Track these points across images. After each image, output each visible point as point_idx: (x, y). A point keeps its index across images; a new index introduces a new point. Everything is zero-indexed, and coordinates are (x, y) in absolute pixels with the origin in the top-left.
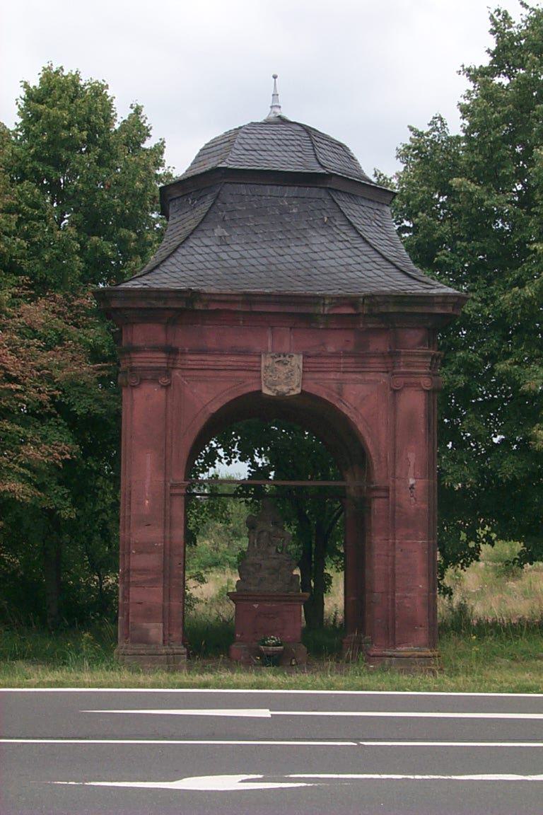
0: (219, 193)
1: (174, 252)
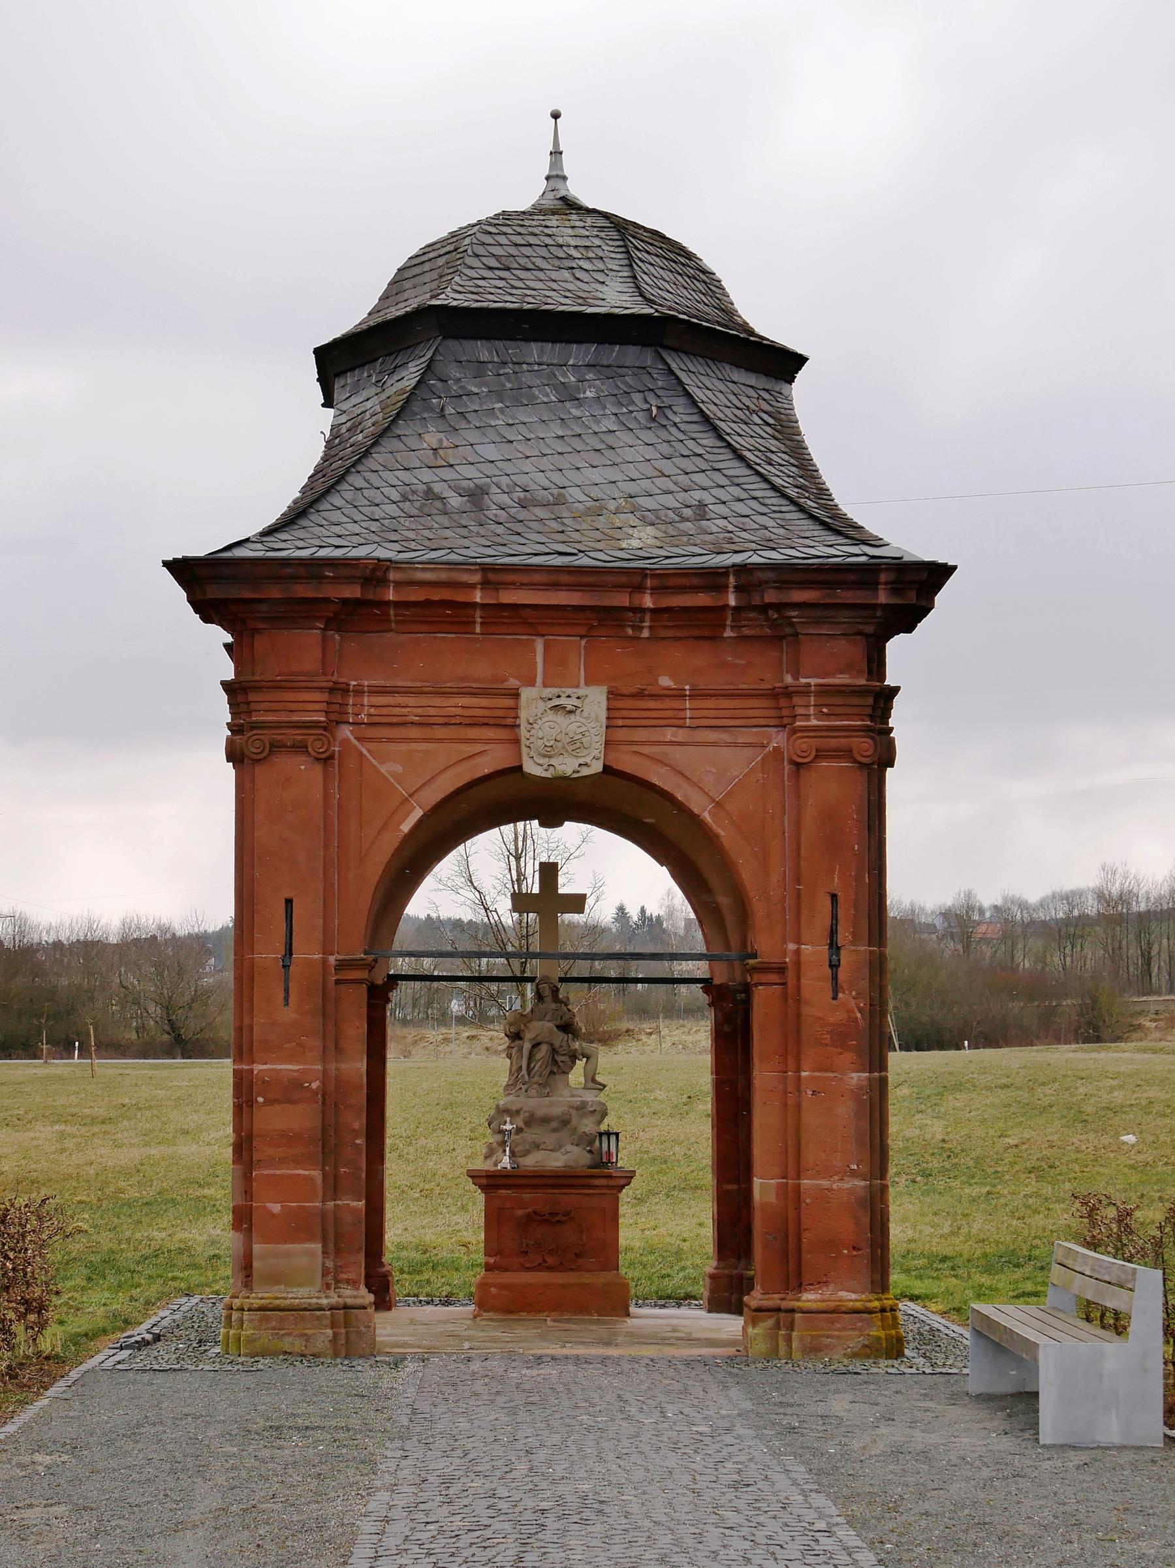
0: (431, 360)
1: (337, 482)
